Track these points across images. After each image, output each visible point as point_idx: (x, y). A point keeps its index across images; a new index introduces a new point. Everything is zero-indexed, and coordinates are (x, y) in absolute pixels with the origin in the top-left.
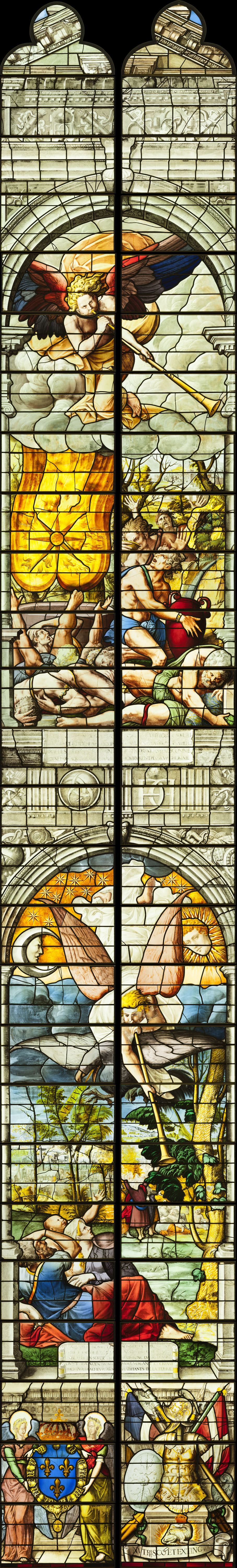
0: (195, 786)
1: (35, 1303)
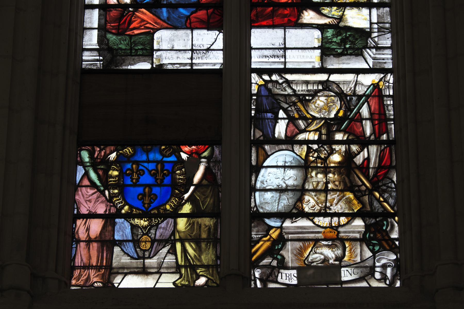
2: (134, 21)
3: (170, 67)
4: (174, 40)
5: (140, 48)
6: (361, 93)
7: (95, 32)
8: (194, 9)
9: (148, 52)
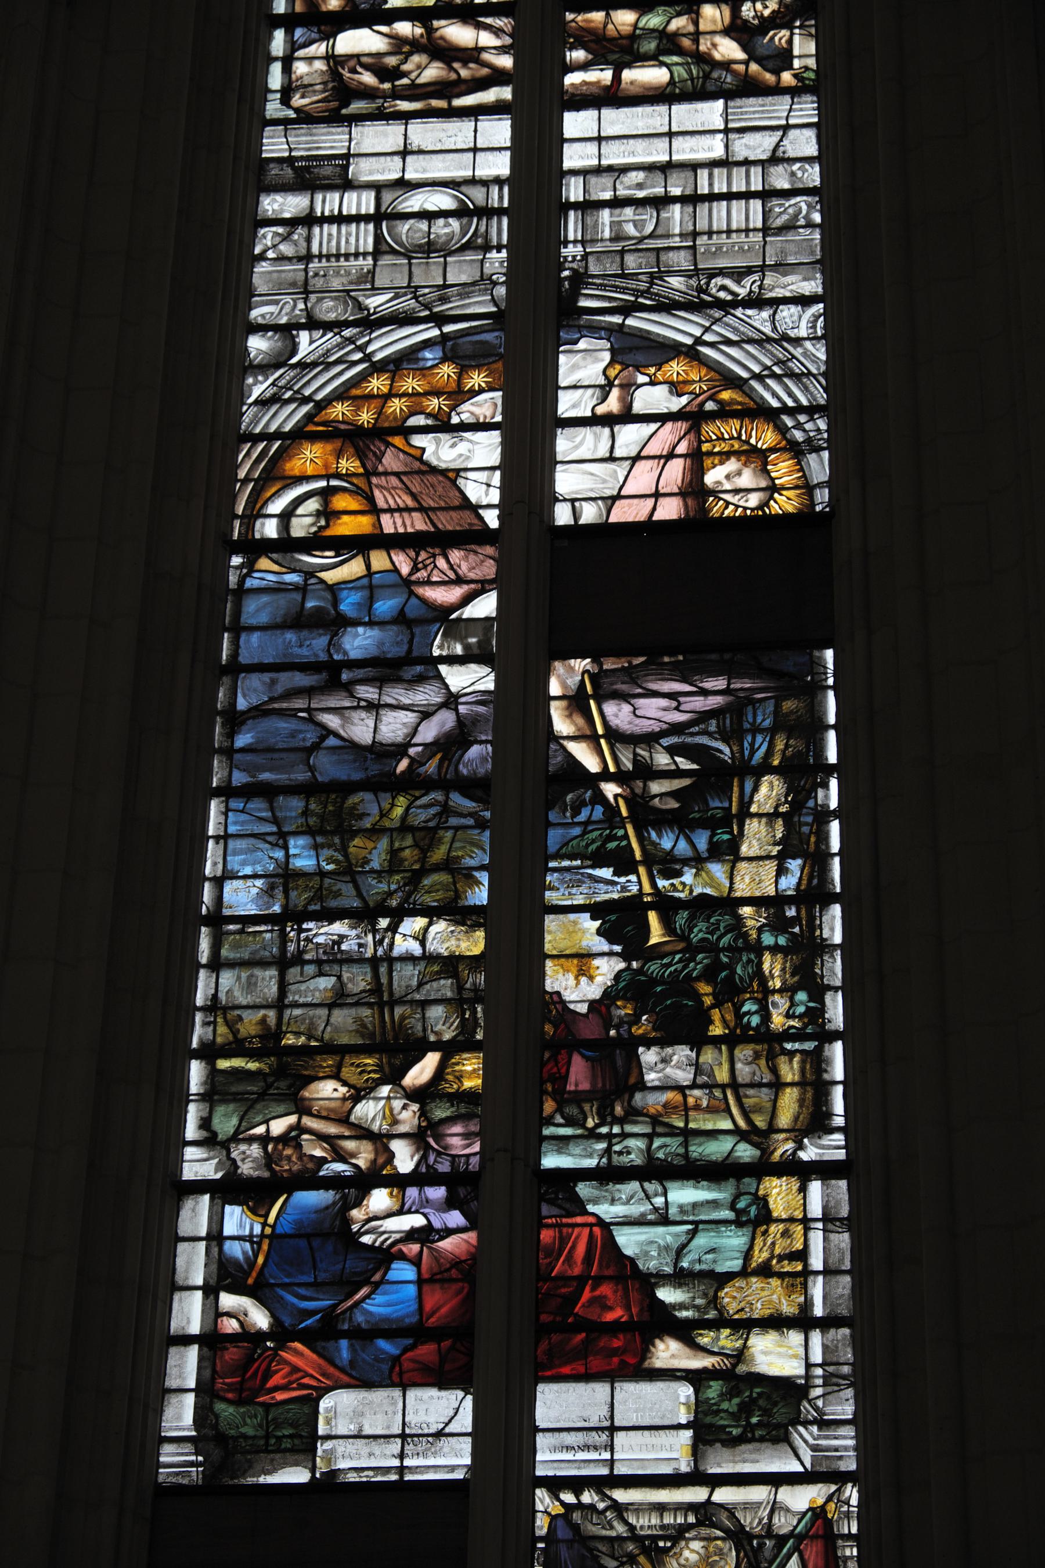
0: (729, 196)
1: (257, 1292)
2: (276, 1372)
3: (352, 1477)
4: (362, 1414)
5: (286, 1433)
6: (784, 1531)
7: (190, 1399)
8: (410, 1341)
9: (305, 1442)
